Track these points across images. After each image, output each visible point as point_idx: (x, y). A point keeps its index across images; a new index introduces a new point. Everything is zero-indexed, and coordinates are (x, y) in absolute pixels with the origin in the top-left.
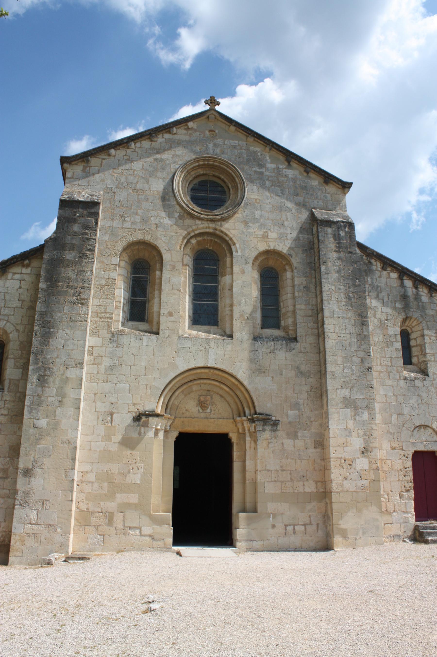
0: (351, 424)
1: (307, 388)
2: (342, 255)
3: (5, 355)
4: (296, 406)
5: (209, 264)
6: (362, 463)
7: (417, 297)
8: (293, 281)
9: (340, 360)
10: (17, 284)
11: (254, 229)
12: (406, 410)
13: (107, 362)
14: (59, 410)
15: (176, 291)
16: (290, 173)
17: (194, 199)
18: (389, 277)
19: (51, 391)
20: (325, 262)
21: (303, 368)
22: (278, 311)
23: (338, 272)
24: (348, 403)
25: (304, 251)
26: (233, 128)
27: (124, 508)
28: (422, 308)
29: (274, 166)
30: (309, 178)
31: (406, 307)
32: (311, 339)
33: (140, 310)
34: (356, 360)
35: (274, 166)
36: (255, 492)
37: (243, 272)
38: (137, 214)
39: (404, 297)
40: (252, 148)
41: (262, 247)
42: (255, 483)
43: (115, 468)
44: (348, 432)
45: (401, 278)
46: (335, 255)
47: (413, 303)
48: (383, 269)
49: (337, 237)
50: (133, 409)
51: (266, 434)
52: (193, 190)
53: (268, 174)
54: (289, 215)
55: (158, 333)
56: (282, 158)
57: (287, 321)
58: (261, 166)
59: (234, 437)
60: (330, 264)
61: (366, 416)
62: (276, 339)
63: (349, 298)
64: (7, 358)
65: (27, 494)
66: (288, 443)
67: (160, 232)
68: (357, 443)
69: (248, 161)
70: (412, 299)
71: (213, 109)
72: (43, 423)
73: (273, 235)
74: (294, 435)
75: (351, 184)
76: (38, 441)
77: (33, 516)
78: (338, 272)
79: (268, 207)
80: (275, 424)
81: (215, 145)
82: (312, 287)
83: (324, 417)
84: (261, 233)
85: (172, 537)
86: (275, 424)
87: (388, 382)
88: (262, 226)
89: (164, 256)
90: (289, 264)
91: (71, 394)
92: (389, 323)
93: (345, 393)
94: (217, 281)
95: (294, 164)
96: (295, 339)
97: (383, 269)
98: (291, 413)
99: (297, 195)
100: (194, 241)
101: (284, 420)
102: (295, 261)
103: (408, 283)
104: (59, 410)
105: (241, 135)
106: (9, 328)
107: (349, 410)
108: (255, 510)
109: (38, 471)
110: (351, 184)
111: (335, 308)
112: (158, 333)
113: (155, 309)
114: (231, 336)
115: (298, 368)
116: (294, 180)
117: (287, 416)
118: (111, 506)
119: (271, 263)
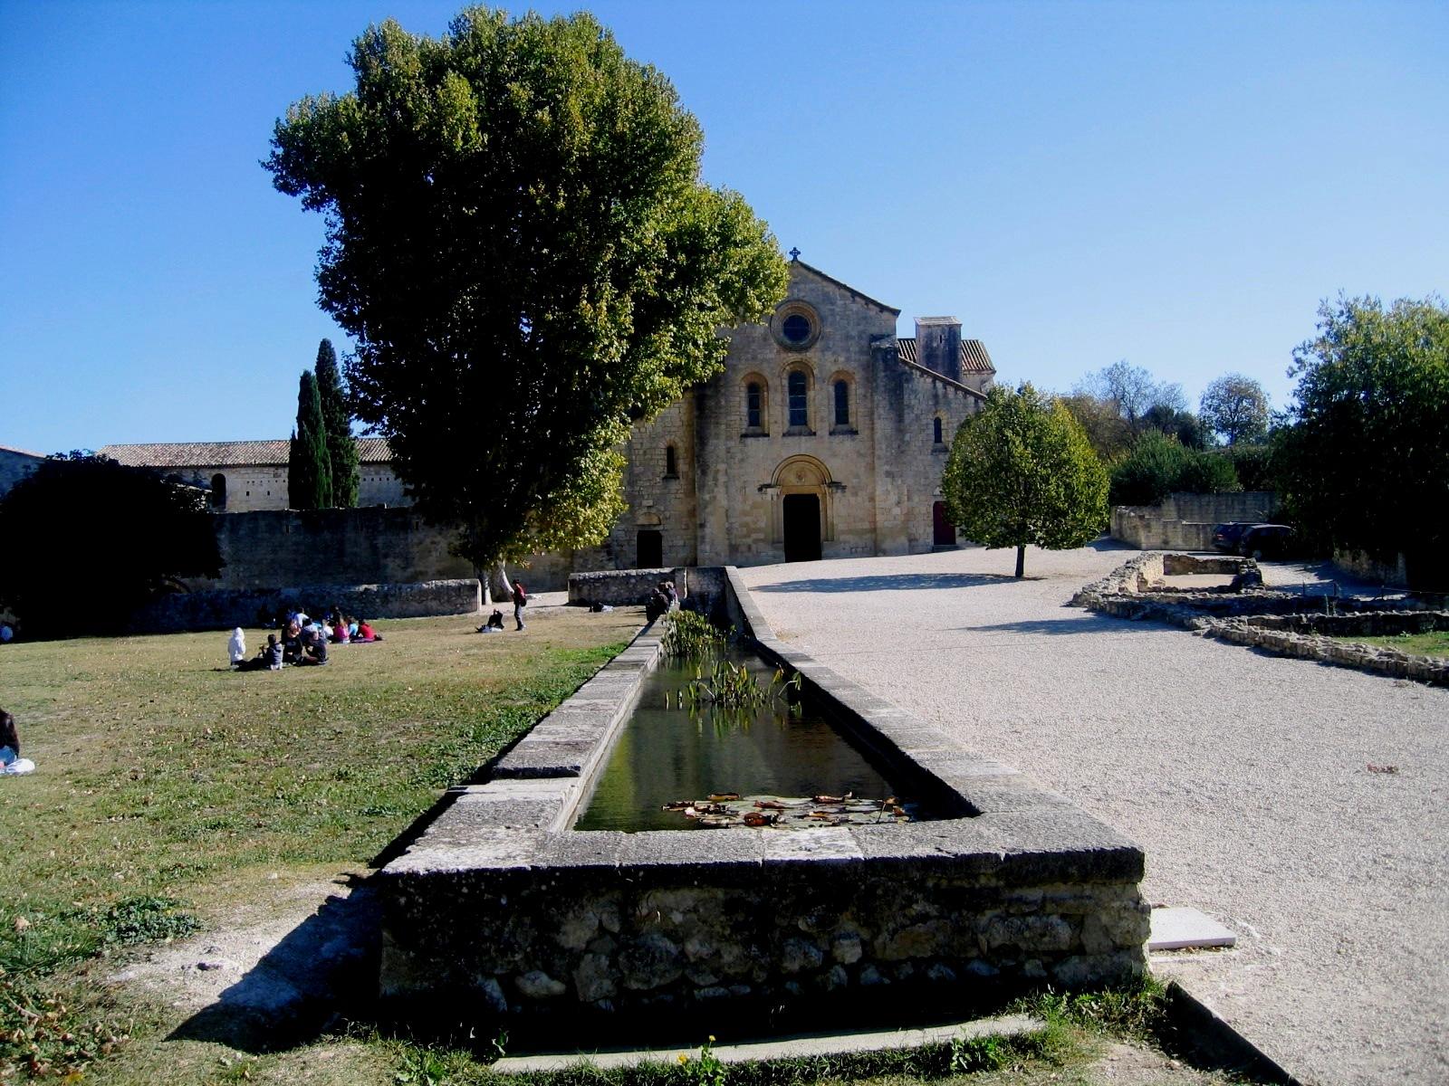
0: (890, 487)
1: (864, 464)
2: (888, 373)
3: (675, 457)
4: (857, 476)
5: (798, 384)
6: (897, 511)
7: (945, 395)
8: (856, 391)
9: (884, 447)
10: (677, 410)
11: (828, 355)
12: (931, 476)
13: (739, 456)
14: (716, 490)
15: (777, 411)
16: (855, 307)
17: (786, 332)
18: (925, 382)
19: (710, 479)
20: (875, 380)
21: (862, 452)
22: (847, 411)
23: (885, 386)
24: (888, 474)
25: (864, 369)
26: (811, 276)
27: (756, 541)
28: (948, 403)
29: (842, 302)
30: (868, 309)
31: (936, 403)
32: (867, 432)
33: (755, 418)
34: (895, 446)
35: (842, 302)
36: (833, 530)
37: (822, 389)
38: (748, 353)
39: (936, 396)
40: (826, 289)
41: (834, 369)
42: (832, 524)
43: (748, 519)
44: (888, 492)
45: (934, 382)
46: (883, 374)
47: (942, 401)
48: (921, 376)
49: (885, 361)
50: (758, 485)
51: (839, 494)
52: (785, 324)
53: (838, 310)
54: (853, 342)
55: (768, 435)
56: (849, 294)
57: (851, 420)
58: (832, 304)
59: (820, 496)
60: (879, 381)
61: (900, 482)
62: (844, 433)
63: (891, 404)
64: (678, 458)
65: (703, 537)
66: (852, 499)
67: (765, 365)
68: (893, 498)
69: (824, 300)
70: (941, 397)
71: (795, 258)
72: (707, 497)
73: (841, 359)
74: (855, 494)
75: (899, 311)
76: (706, 507)
77: (708, 548)
78: (885, 386)
79: (838, 337)
80: (844, 488)
81: (799, 290)
82: (869, 395)
83: (874, 481)
84: (833, 359)
85: (782, 545)
86: (844, 488)
87: (920, 457)
88: (834, 353)
89: (770, 383)
90: (853, 378)
91: (722, 479)
92: (922, 417)
93: (887, 468)
94: (805, 394)
95: (858, 299)
96: (856, 433)
97: (921, 376)
98: (854, 481)
99: (859, 325)
100: (788, 368)
101: (849, 485)
102: (857, 377)
103: (939, 385)
104: (716, 490)
105: (818, 278)
106: (677, 440)
107: (889, 480)
108: (833, 540)
109: (708, 525)
110: (899, 311)
111: (882, 412)
112: (768, 435)
113: (766, 418)
114: (815, 434)
115: (858, 452)
116: (857, 313)
117: (850, 482)
118: (749, 541)
119: (841, 377)
